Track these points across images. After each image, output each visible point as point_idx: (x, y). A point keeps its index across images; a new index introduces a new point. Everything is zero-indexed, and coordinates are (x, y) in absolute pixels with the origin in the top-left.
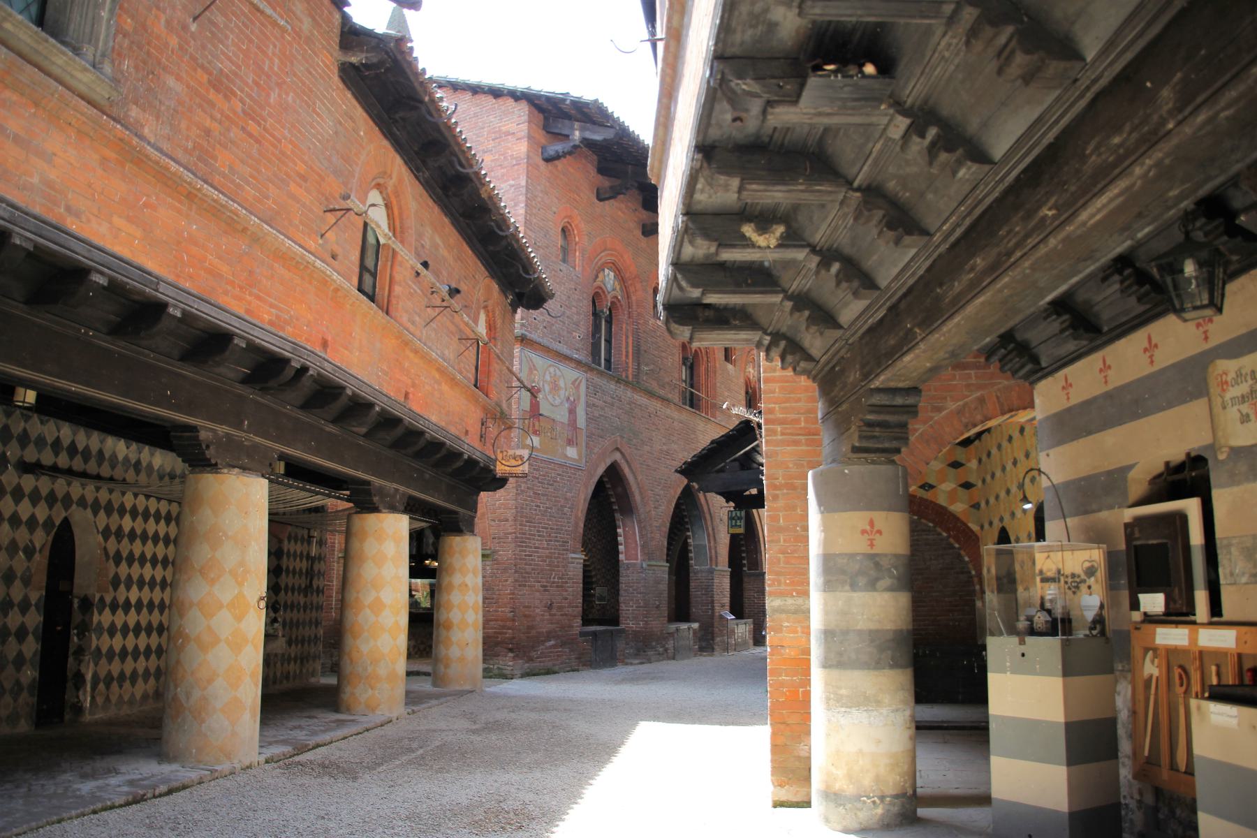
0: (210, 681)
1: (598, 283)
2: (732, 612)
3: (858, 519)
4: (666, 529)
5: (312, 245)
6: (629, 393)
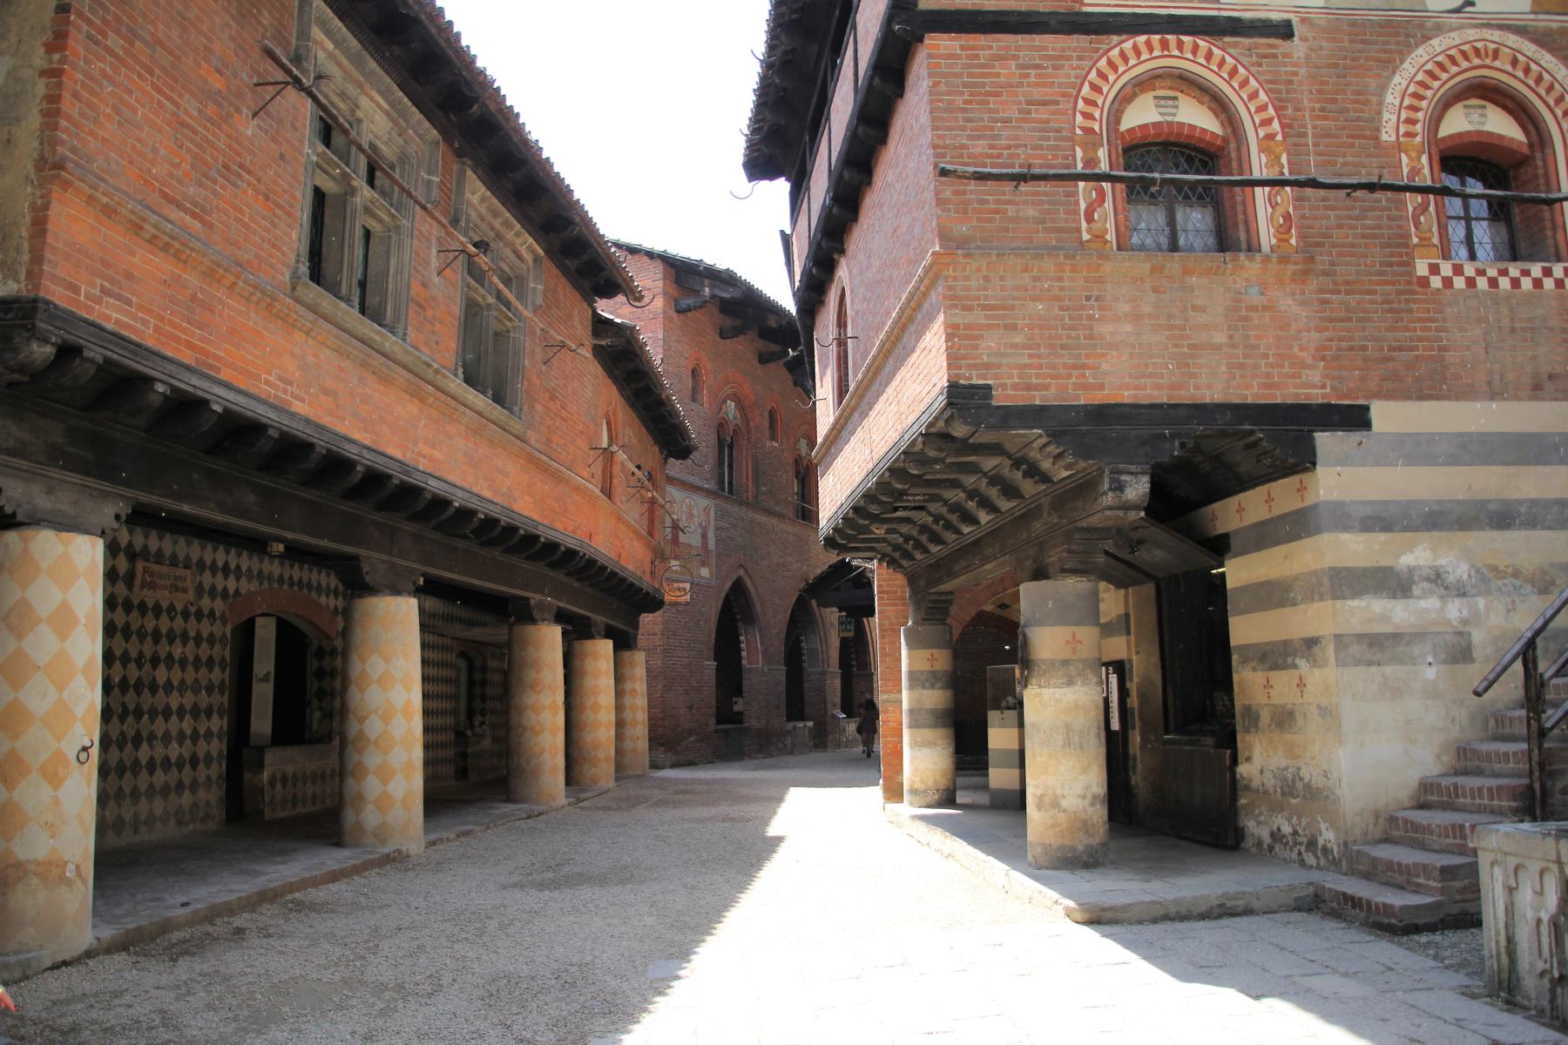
0: (541, 753)
1: (722, 415)
2: (843, 711)
3: (925, 653)
4: (783, 636)
5: (586, 474)
6: (750, 513)
